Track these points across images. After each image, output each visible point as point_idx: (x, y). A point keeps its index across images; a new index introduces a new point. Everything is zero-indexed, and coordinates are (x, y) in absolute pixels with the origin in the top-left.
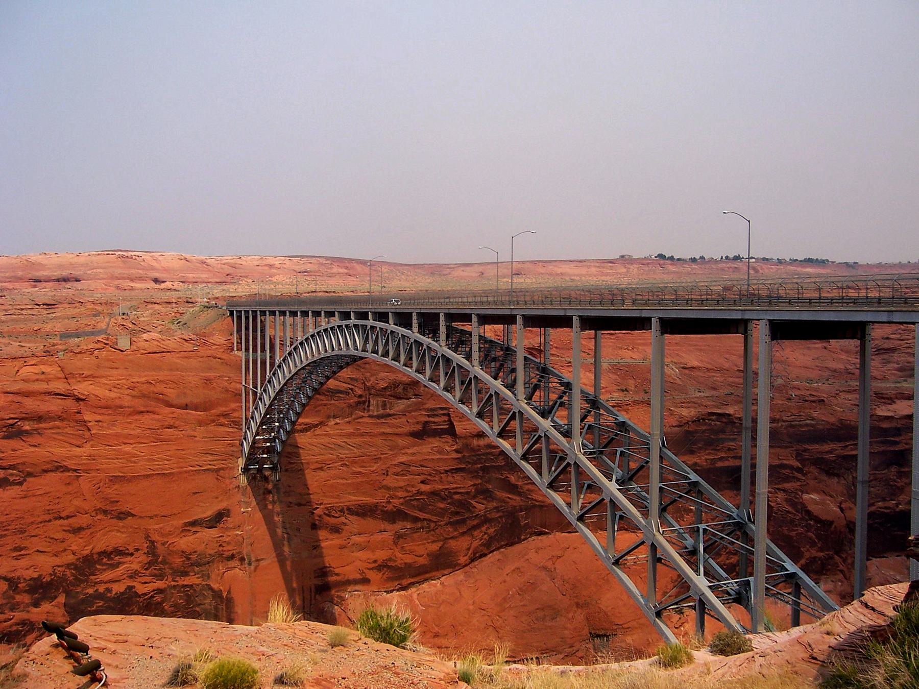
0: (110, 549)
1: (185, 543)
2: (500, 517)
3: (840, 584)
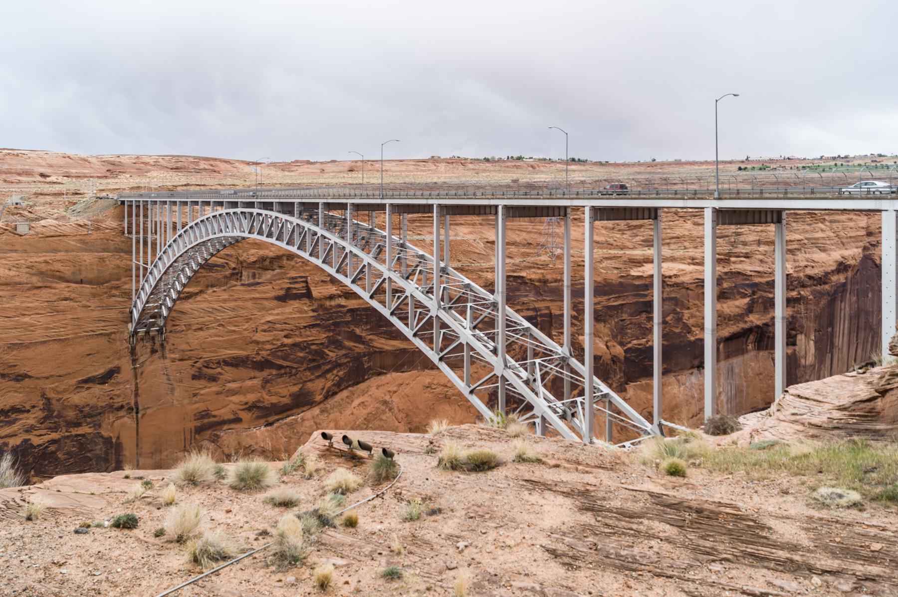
0: (8, 407)
1: (77, 398)
2: (348, 362)
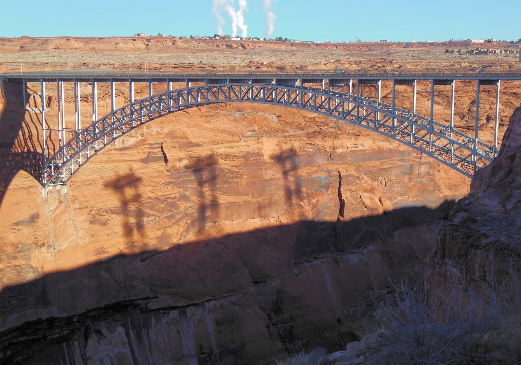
1: (12, 237)
3: (381, 246)
